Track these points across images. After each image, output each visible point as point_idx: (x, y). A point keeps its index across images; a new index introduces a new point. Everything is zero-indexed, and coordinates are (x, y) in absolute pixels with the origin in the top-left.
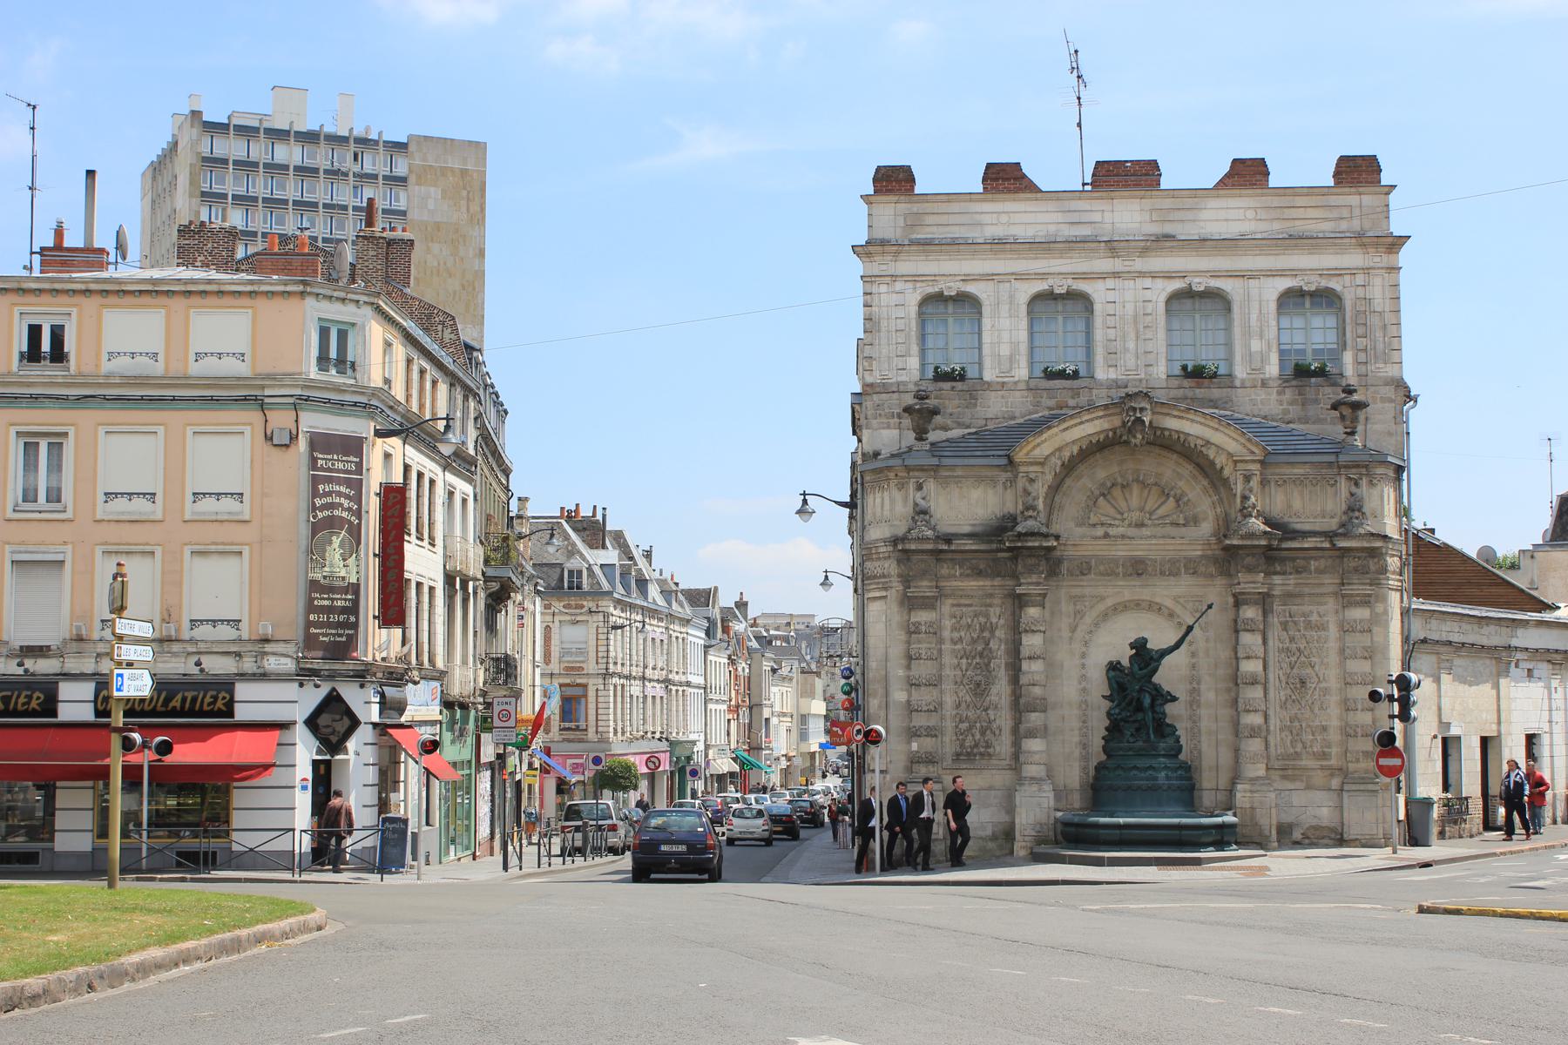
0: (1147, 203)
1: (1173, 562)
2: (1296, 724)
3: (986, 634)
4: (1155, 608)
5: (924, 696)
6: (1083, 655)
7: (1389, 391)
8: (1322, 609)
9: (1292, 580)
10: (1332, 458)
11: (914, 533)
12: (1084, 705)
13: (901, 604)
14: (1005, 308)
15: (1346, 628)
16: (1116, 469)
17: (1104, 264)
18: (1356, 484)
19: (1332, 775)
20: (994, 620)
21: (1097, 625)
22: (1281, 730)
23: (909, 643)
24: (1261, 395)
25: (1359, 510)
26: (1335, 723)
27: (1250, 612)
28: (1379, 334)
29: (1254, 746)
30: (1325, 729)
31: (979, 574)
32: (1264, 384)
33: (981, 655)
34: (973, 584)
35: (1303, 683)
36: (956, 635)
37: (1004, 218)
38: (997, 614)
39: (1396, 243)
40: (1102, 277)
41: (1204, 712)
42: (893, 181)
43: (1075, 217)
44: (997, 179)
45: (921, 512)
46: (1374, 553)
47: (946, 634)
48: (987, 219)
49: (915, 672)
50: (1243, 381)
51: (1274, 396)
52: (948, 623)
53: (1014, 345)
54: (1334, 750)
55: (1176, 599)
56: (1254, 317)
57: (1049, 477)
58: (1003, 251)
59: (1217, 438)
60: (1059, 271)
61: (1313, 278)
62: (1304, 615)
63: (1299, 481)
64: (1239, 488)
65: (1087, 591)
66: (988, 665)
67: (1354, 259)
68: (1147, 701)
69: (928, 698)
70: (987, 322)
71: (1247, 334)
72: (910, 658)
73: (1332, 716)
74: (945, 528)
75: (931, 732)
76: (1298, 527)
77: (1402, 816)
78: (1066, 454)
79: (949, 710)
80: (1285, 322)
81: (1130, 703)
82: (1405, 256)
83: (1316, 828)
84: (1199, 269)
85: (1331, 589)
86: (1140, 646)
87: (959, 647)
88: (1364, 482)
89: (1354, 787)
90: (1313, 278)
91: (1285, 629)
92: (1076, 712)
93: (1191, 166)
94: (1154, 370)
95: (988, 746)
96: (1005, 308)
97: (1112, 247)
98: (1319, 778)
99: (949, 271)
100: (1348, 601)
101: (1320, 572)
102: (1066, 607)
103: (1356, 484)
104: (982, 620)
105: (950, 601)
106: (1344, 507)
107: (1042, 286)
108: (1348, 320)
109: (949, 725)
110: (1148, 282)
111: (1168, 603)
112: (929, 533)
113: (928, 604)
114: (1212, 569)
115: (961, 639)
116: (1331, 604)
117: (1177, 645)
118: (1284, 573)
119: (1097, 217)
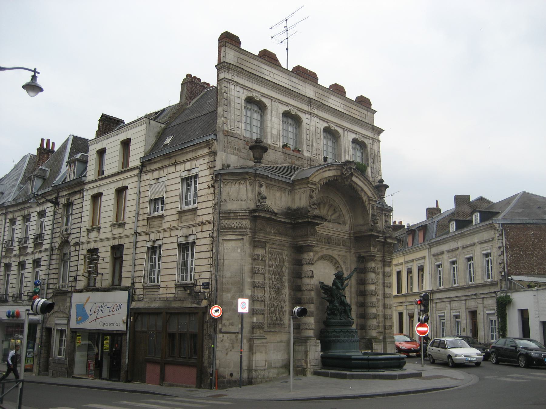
13: (250, 244)
14: (275, 113)
17: (305, 107)
28: (377, 163)
33: (279, 273)
37: (272, 75)
38: (286, 255)
39: (380, 131)
40: (305, 112)
42: (228, 40)
43: (294, 85)
48: (266, 72)
52: (267, 256)
53: (278, 131)
66: (281, 279)
67: (369, 134)
82: (382, 137)
87: (271, 269)
95: (281, 320)
97: (310, 101)
110: (318, 120)
115: (272, 265)
116: (380, 265)
119: (300, 87)
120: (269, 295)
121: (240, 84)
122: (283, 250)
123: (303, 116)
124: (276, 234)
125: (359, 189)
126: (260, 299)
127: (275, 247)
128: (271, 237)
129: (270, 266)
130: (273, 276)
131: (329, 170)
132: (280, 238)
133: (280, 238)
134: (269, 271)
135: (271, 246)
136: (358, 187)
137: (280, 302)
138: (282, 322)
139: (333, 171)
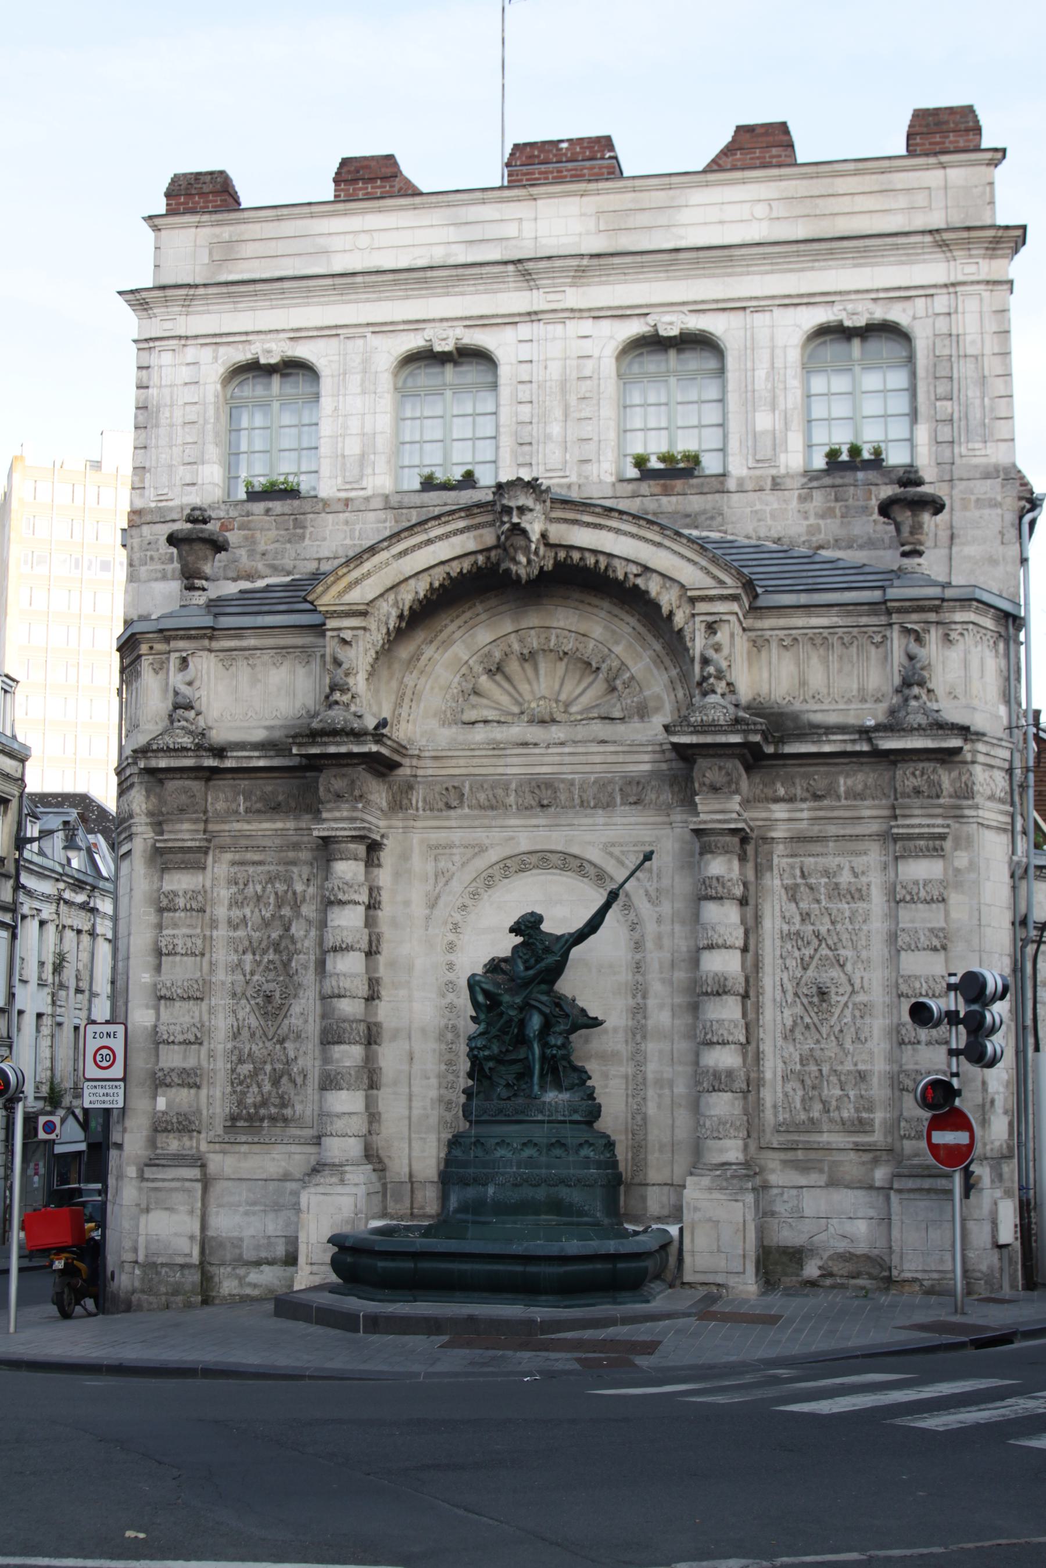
0: (591, 203)
1: (602, 785)
2: (813, 1068)
3: (286, 911)
5: (179, 1017)
6: (451, 947)
7: (990, 488)
8: (860, 862)
9: (805, 811)
10: (876, 595)
11: (169, 741)
12: (446, 1033)
14: (354, 381)
15: (898, 898)
16: (508, 626)
17: (515, 299)
18: (919, 639)
19: (876, 1161)
20: (299, 887)
21: (475, 895)
22: (785, 1079)
23: (160, 927)
24: (771, 501)
25: (921, 684)
26: (879, 1066)
27: (720, 866)
28: (973, 392)
29: (722, 1105)
30: (862, 1077)
31: (274, 809)
32: (776, 485)
34: (267, 827)
35: (822, 994)
36: (236, 913)
37: (363, 240)
40: (511, 320)
41: (651, 1047)
44: (355, 181)
45: (182, 705)
46: (947, 757)
47: (221, 912)
48: (337, 243)
49: (166, 977)
50: (741, 481)
51: (794, 504)
53: (368, 439)
54: (879, 1116)
55: (607, 848)
56: (761, 374)
57: (377, 636)
58: (353, 287)
59: (661, 559)
60: (443, 316)
61: (860, 307)
62: (826, 873)
63: (820, 640)
64: (698, 644)
65: (456, 836)
66: (286, 965)
67: (932, 270)
68: (536, 1022)
69: (186, 1020)
70: (326, 402)
71: (750, 404)
72: (159, 953)
73: (875, 1055)
74: (219, 736)
75: (190, 1079)
76: (818, 718)
77: (1007, 1234)
78: (407, 596)
79: (220, 1040)
80: (818, 384)
81: (503, 1031)
83: (847, 1257)
84: (670, 300)
85: (874, 827)
86: (528, 927)
87: (241, 933)
88: (934, 636)
89: (910, 1184)
90: (860, 307)
91: (793, 899)
92: (434, 1045)
93: (665, 135)
94: (592, 470)
95: (284, 1105)
96: (354, 381)
97: (524, 269)
98: (851, 1165)
99: (269, 327)
100: (899, 844)
101: (853, 795)
102: (417, 862)
103: (919, 639)
104: (281, 887)
105: (229, 856)
106: (897, 681)
107: (414, 342)
108: (921, 372)
109: (221, 1066)
110: (587, 326)
111: (594, 855)
112: (186, 741)
113: (191, 859)
114: (667, 796)
116: (873, 856)
117: (593, 925)
118: (791, 800)
119: (511, 230)
120: (231, 1020)
121: (196, 337)
122: (294, 863)
123: (498, 342)
124: (259, 811)
125: (620, 570)
126: (180, 1038)
127: (256, 857)
128: (237, 826)
129: (233, 925)
130: (249, 957)
131: (429, 542)
132: (279, 825)
133: (279, 825)
134: (232, 941)
135: (237, 857)
136: (616, 563)
137: (282, 1042)
138: (288, 1112)
139: (455, 540)
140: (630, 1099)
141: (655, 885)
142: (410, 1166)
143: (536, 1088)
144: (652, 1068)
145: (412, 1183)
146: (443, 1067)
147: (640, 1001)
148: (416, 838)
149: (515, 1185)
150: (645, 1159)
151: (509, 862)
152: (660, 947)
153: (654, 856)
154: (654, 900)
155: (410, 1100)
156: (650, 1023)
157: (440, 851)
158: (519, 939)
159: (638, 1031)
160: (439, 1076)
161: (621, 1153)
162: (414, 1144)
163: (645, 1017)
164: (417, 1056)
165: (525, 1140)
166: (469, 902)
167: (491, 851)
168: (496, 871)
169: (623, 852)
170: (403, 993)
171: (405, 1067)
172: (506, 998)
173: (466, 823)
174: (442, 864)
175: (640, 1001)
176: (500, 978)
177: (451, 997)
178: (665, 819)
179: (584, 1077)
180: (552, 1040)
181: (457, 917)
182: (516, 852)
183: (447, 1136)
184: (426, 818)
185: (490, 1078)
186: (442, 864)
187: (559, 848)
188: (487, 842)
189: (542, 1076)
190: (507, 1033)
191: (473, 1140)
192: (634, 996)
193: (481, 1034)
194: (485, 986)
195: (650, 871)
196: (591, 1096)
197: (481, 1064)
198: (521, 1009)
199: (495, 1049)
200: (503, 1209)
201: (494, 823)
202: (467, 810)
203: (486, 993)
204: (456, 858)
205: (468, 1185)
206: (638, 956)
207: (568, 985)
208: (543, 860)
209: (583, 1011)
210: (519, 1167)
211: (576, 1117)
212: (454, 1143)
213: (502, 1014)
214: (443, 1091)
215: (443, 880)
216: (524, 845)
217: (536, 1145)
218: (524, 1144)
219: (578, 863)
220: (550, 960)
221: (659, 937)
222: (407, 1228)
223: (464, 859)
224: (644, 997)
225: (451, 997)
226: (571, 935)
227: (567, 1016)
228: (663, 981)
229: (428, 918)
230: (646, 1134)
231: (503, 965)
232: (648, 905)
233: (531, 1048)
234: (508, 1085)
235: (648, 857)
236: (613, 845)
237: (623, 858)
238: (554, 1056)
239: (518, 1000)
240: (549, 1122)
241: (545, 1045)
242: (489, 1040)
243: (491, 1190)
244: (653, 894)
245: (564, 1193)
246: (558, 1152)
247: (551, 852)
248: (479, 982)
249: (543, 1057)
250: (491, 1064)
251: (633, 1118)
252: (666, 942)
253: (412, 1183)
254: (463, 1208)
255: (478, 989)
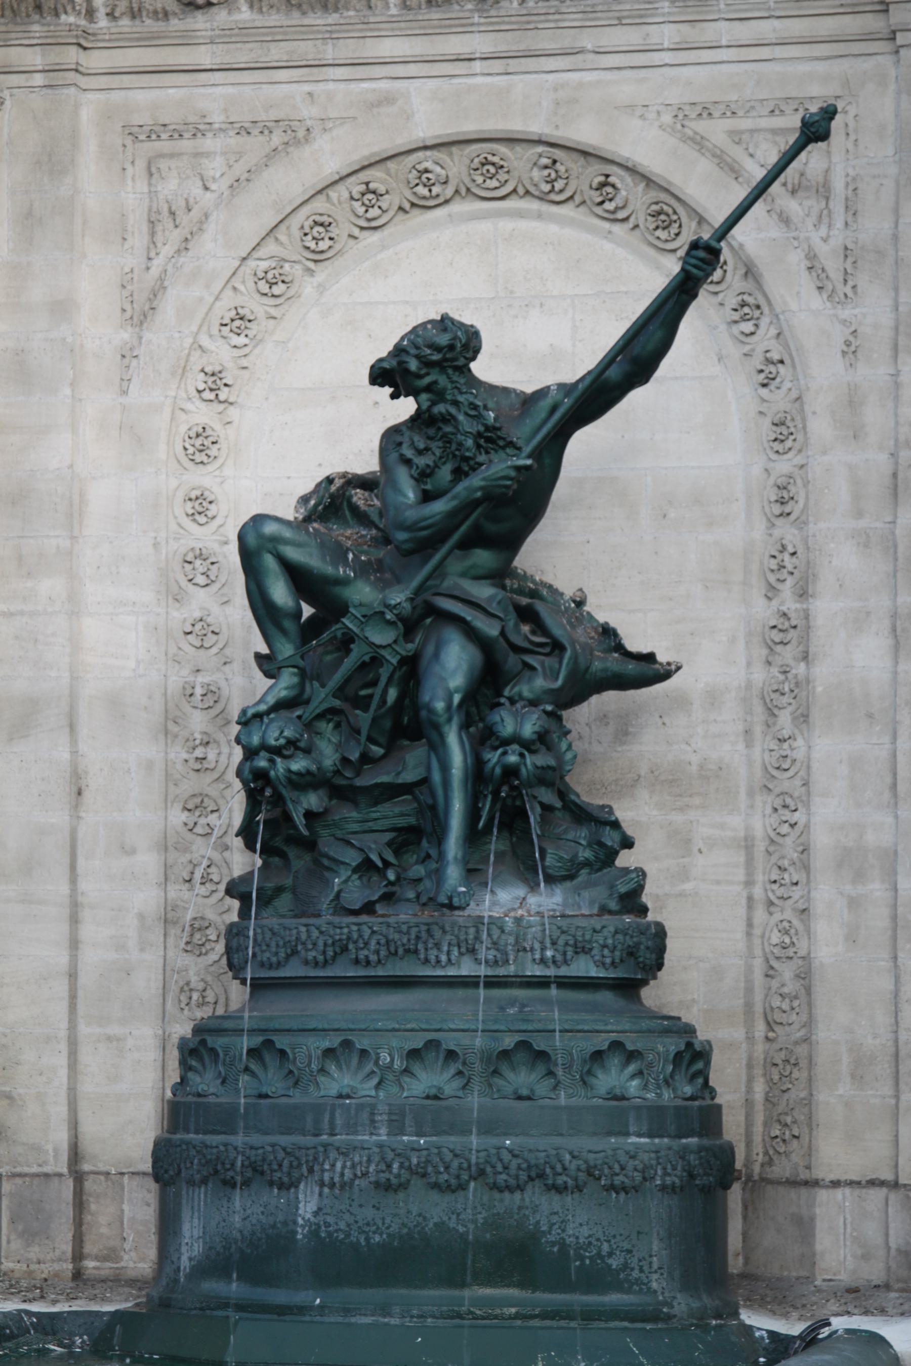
4: (577, 177)
6: (201, 446)
21: (273, 284)
41: (827, 749)
65: (214, 98)
68: (453, 665)
81: (352, 695)
92: (152, 751)
111: (644, 144)
117: (637, 358)
140: (760, 914)
141: (838, 237)
142: (74, 1125)
143: (453, 873)
144: (828, 816)
145: (79, 1178)
146: (178, 817)
147: (791, 605)
148: (88, 107)
149: (387, 1187)
150: (808, 1102)
151: (378, 178)
152: (856, 434)
153: (836, 124)
154: (835, 283)
155: (74, 920)
156: (823, 674)
157: (165, 146)
158: (407, 407)
159: (785, 702)
160: (164, 846)
161: (730, 1081)
162: (86, 1056)
163: (805, 657)
164: (94, 782)
165: (418, 1042)
166: (255, 306)
167: (322, 142)
168: (339, 206)
169: (736, 136)
170: (51, 586)
171: (59, 818)
172: (362, 593)
173: (242, 55)
174: (169, 187)
175: (791, 605)
176: (347, 533)
177: (200, 601)
178: (873, 23)
179: (610, 838)
180: (506, 722)
181: (221, 353)
182: (402, 141)
183: (183, 1029)
184: (117, 43)
185: (310, 845)
186: (169, 187)
187: (536, 127)
188: (309, 112)
189: (474, 835)
190: (363, 703)
191: (245, 1043)
192: (771, 592)
193: (281, 706)
194: (292, 553)
195: (824, 191)
196: (632, 901)
197: (278, 800)
198: (409, 626)
199: (328, 752)
200: (344, 1263)
201: (330, 53)
202: (245, 14)
203: (298, 577)
204: (214, 167)
205: (230, 1184)
206: (784, 466)
207: (561, 553)
208: (488, 168)
209: (608, 632)
210: (397, 1128)
211: (584, 967)
212: (197, 1051)
213: (346, 642)
214: (176, 891)
215: (176, 236)
216: (427, 124)
217: (451, 1055)
218: (414, 1054)
219: (593, 173)
220: (499, 467)
221: (853, 401)
222: (49, 1325)
223: (239, 169)
224: (803, 594)
225: (200, 601)
226: (566, 389)
227: (557, 647)
228: (864, 540)
229: (127, 355)
230: (809, 1024)
231: (359, 497)
232: (817, 302)
233: (438, 747)
234: (366, 867)
235: (815, 130)
236: (706, 112)
237: (737, 153)
238: (511, 772)
239: (399, 597)
240: (492, 983)
241: (483, 738)
242: (309, 726)
243: (307, 1204)
244: (833, 267)
245: (542, 1210)
246: (522, 1078)
247: (511, 141)
248: (275, 539)
249: (478, 775)
250: (313, 800)
251: (770, 973)
252: (875, 417)
253: (79, 1178)
254: (216, 1265)
255: (270, 562)
